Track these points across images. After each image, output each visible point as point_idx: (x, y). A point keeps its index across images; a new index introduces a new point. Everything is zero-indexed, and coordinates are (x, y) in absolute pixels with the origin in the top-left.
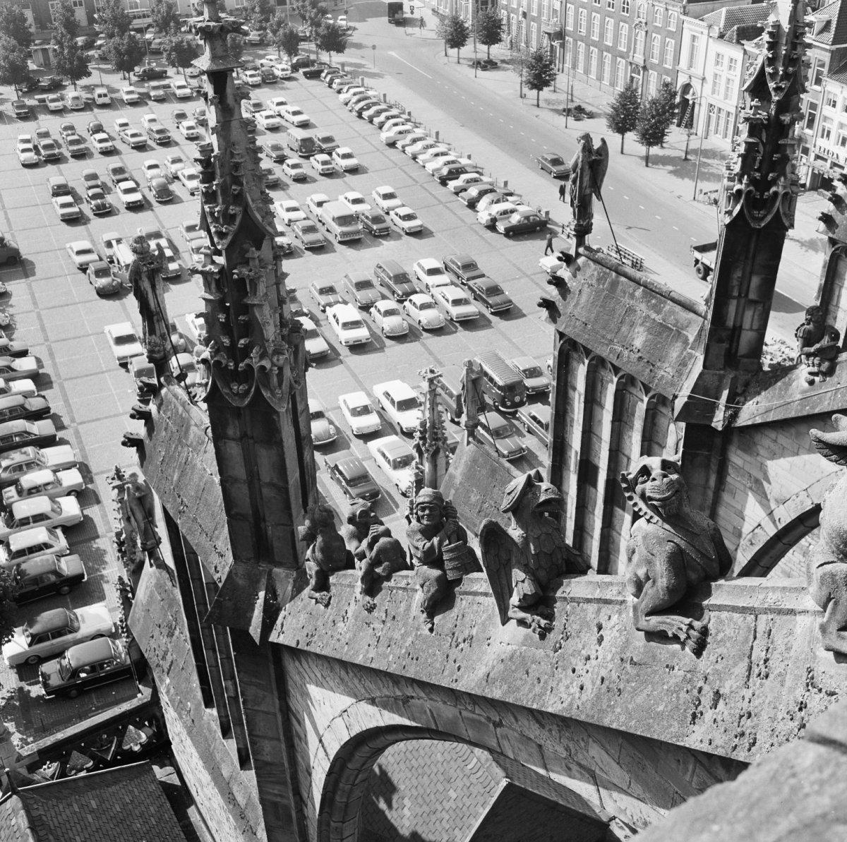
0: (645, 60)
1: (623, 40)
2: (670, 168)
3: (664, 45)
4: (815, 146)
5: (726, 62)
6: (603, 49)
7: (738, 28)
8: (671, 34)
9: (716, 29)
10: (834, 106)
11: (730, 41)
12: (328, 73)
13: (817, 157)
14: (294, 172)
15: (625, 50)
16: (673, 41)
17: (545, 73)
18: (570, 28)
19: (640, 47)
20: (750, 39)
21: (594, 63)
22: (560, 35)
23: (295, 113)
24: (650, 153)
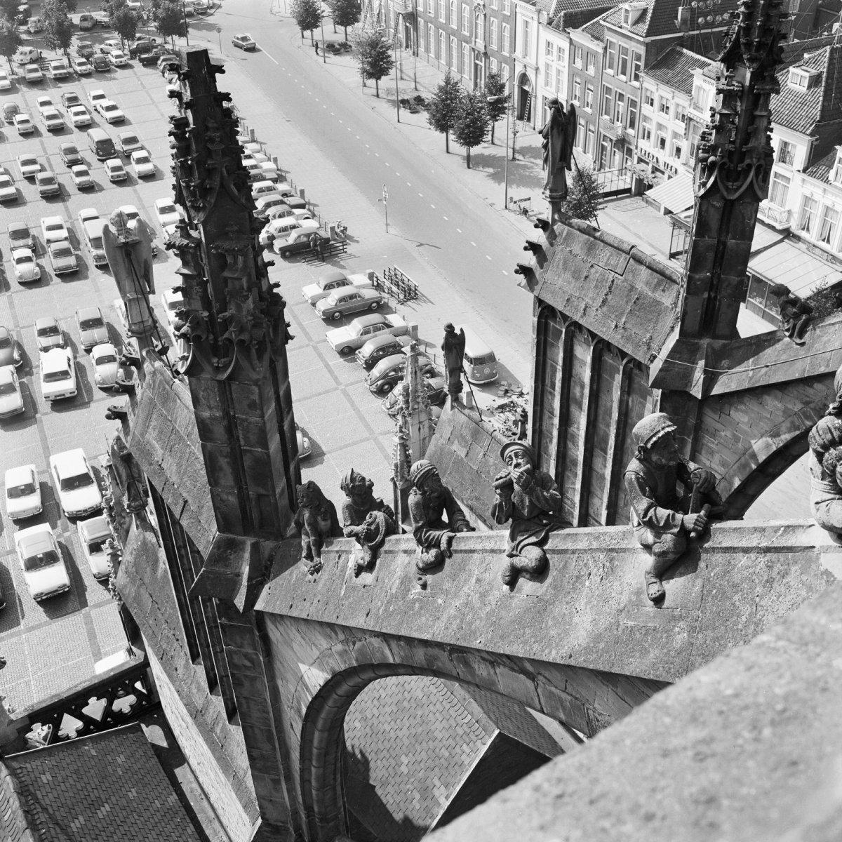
0: (485, 46)
1: (466, 24)
2: (491, 170)
3: (501, 30)
4: (636, 148)
5: (555, 50)
6: (450, 33)
7: (565, 14)
8: (505, 19)
9: (545, 13)
10: (652, 104)
11: (557, 27)
12: (164, 60)
13: (640, 160)
14: (78, 180)
15: (468, 34)
16: (509, 26)
17: (382, 61)
18: (420, 9)
19: (480, 31)
20: (575, 27)
21: (443, 46)
22: (412, 17)
23: (109, 109)
24: (471, 154)
